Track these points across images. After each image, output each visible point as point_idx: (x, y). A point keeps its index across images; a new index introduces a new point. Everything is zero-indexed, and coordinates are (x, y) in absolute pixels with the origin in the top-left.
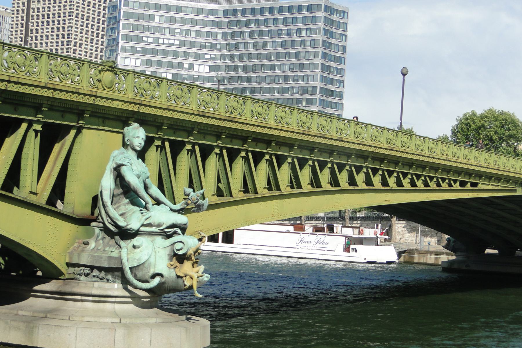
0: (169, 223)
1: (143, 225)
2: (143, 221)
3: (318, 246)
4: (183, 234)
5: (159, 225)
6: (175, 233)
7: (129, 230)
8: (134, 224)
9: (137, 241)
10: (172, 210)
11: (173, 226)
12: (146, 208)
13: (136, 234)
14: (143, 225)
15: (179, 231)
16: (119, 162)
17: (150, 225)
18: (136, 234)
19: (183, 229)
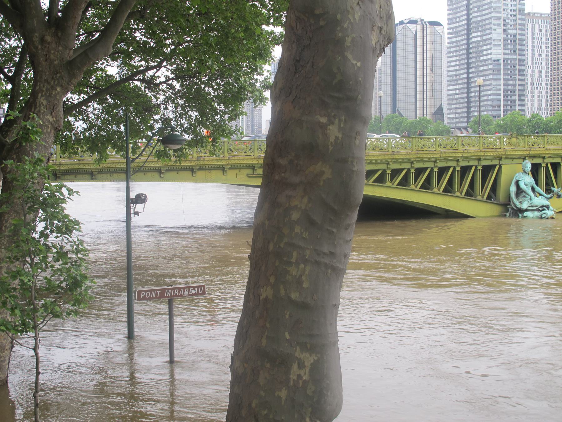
0: (541, 205)
1: (529, 207)
2: (528, 205)
4: (548, 210)
5: (536, 206)
6: (544, 210)
7: (523, 209)
8: (525, 206)
9: (525, 214)
10: (546, 198)
11: (543, 206)
12: (530, 199)
13: (526, 210)
14: (529, 207)
15: (546, 209)
16: (518, 179)
17: (532, 206)
18: (526, 210)
19: (548, 207)
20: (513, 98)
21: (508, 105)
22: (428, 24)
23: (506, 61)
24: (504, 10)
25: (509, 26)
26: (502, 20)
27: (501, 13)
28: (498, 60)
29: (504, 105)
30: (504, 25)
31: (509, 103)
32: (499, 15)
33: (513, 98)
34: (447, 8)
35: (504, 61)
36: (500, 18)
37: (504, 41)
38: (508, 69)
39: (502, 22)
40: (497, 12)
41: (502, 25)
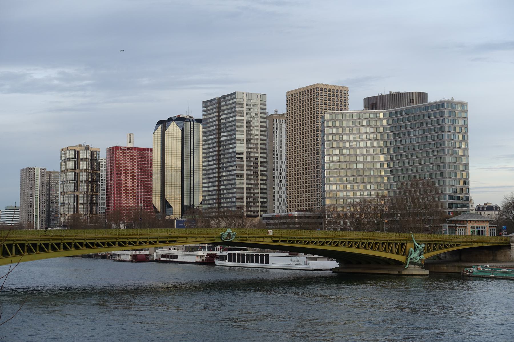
3: (297, 263)
20: (256, 191)
21: (251, 197)
22: (195, 121)
23: (248, 158)
24: (247, 113)
25: (252, 128)
26: (245, 122)
27: (243, 116)
28: (242, 158)
29: (247, 198)
30: (247, 127)
31: (252, 195)
32: (242, 118)
33: (256, 191)
34: (202, 109)
35: (247, 158)
36: (243, 120)
37: (247, 140)
38: (251, 166)
39: (245, 124)
40: (241, 116)
41: (245, 127)
